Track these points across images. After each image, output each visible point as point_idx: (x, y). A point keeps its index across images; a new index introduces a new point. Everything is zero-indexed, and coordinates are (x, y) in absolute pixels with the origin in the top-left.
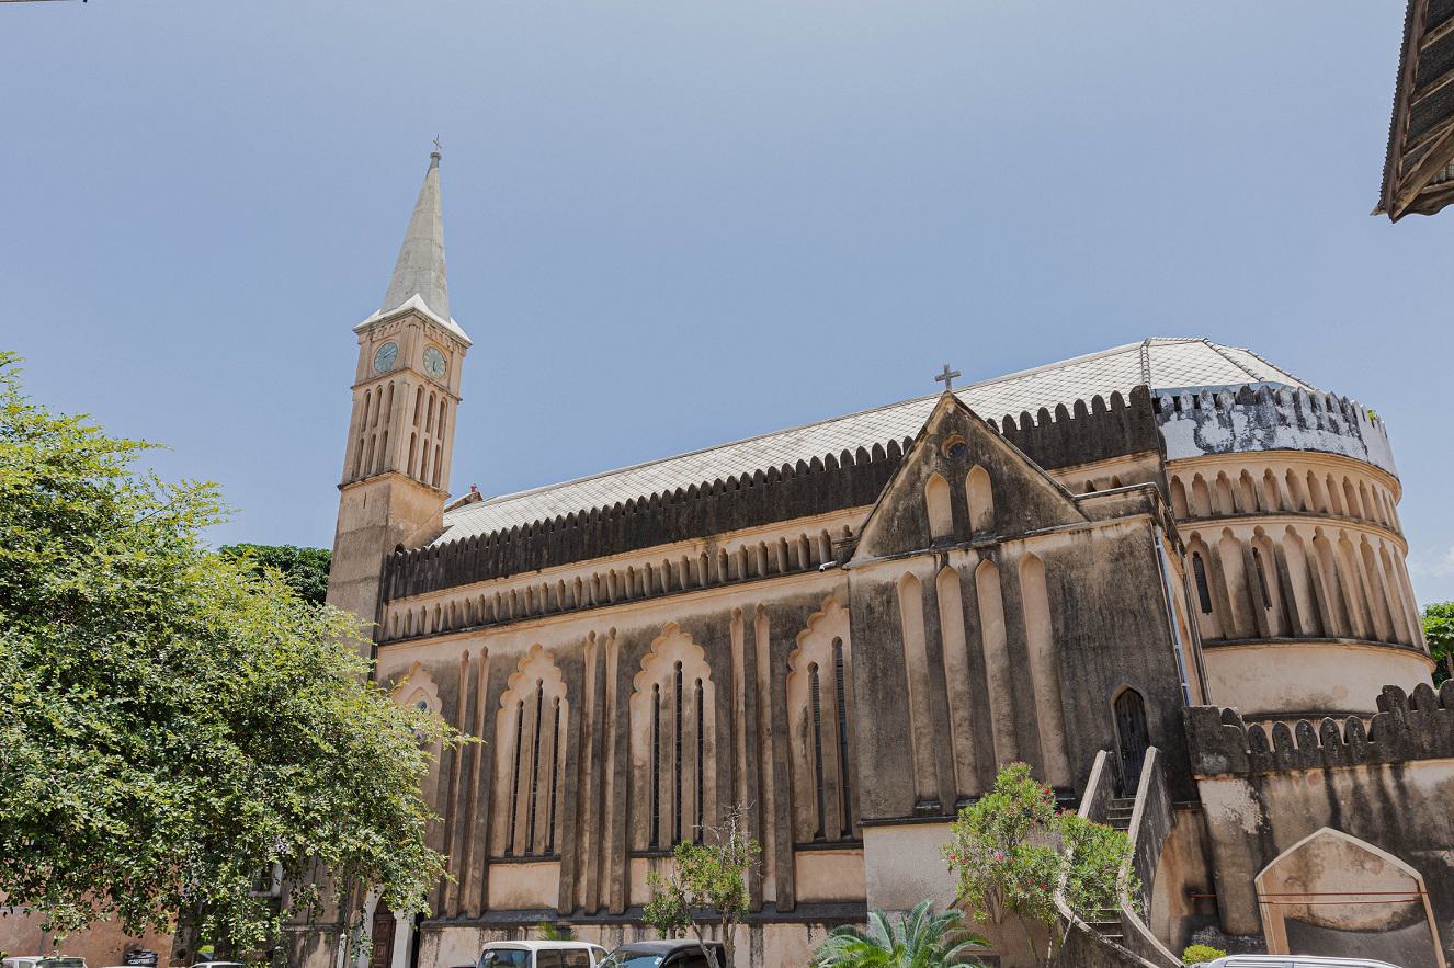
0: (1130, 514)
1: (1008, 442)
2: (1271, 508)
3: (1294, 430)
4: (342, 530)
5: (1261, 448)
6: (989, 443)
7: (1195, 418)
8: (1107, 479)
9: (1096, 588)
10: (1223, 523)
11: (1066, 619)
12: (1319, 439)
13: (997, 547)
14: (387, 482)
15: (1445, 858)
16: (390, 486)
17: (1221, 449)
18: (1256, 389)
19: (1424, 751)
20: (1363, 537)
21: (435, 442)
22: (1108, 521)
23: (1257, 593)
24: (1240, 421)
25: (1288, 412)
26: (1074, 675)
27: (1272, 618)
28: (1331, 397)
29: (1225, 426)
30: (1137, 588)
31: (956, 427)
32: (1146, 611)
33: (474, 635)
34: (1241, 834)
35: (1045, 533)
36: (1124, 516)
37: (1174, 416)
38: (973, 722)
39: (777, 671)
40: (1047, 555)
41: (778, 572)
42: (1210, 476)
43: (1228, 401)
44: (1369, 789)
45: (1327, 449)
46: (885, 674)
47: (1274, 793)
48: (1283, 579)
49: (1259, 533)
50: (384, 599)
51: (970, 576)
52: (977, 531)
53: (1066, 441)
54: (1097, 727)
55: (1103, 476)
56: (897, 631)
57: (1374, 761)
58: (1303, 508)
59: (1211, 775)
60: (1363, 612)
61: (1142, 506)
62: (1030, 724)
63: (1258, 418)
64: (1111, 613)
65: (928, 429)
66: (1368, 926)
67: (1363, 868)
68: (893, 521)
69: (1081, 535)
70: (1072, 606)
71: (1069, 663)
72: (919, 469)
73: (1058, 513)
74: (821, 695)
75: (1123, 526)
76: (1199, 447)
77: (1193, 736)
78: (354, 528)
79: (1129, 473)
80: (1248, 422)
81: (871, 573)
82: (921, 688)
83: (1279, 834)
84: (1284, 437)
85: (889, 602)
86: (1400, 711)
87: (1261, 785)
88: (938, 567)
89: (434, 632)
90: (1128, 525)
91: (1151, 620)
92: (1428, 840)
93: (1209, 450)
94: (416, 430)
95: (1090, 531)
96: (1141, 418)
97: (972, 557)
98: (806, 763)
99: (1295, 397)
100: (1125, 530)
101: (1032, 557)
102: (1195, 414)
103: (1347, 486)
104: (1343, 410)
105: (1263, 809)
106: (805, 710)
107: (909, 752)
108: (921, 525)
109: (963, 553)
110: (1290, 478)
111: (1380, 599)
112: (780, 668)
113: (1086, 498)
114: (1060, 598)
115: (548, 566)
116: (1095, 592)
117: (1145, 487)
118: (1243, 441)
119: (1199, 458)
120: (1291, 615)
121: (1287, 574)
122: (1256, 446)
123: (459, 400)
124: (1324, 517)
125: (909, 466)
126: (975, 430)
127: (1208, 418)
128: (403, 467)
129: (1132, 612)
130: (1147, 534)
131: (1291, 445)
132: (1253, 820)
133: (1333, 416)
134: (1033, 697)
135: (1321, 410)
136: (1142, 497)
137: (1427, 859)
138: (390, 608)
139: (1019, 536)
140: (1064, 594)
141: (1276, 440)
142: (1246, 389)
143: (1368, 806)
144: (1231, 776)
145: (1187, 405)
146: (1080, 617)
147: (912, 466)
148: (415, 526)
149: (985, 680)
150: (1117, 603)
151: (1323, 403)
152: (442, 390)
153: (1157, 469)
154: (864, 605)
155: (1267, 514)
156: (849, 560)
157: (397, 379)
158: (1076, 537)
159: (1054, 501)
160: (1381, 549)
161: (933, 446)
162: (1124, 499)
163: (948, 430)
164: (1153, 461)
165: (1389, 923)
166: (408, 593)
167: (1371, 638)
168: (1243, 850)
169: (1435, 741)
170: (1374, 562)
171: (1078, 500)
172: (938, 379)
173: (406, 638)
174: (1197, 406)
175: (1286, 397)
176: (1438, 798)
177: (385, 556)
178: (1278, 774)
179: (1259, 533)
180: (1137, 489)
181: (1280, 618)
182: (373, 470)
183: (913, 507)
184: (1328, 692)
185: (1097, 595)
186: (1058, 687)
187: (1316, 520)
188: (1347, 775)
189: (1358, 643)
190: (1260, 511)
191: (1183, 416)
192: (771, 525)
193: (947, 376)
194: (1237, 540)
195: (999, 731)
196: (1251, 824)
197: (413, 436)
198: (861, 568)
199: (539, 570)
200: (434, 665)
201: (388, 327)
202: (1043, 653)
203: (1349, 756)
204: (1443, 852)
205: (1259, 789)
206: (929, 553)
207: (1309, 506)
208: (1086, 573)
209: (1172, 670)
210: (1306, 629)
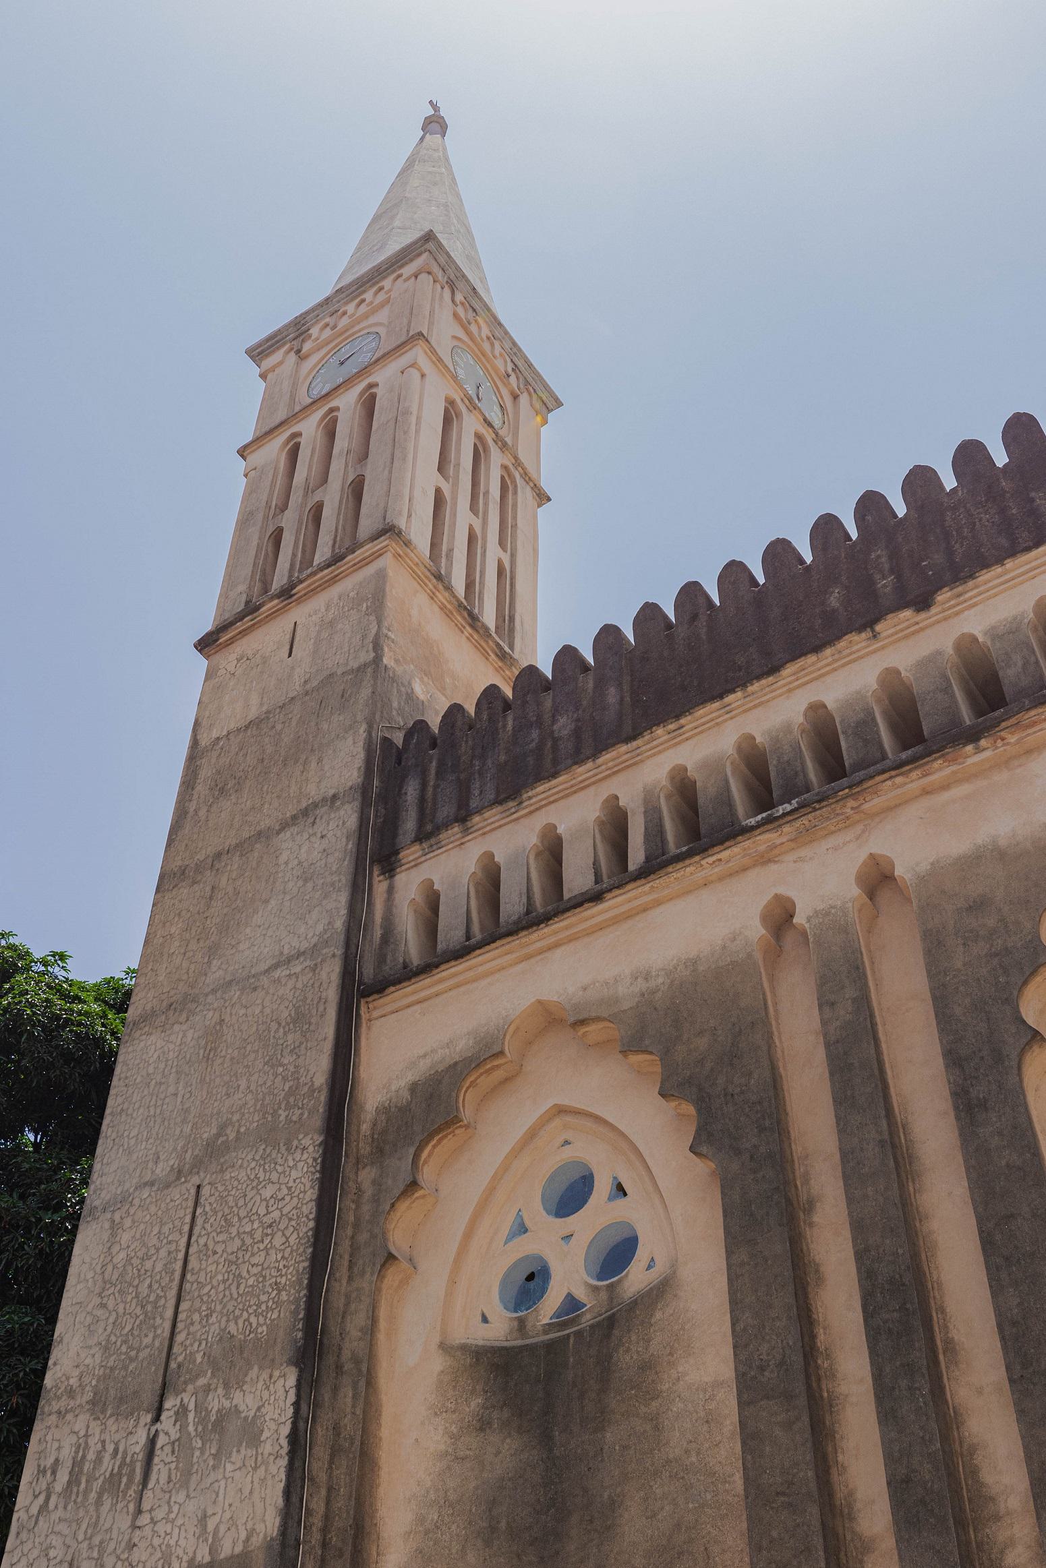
4: (204, 741)
16: (381, 576)
33: (798, 840)
78: (253, 713)
138: (401, 878)
157: (383, 376)
166: (474, 803)
182: (323, 553)
201: (350, 308)
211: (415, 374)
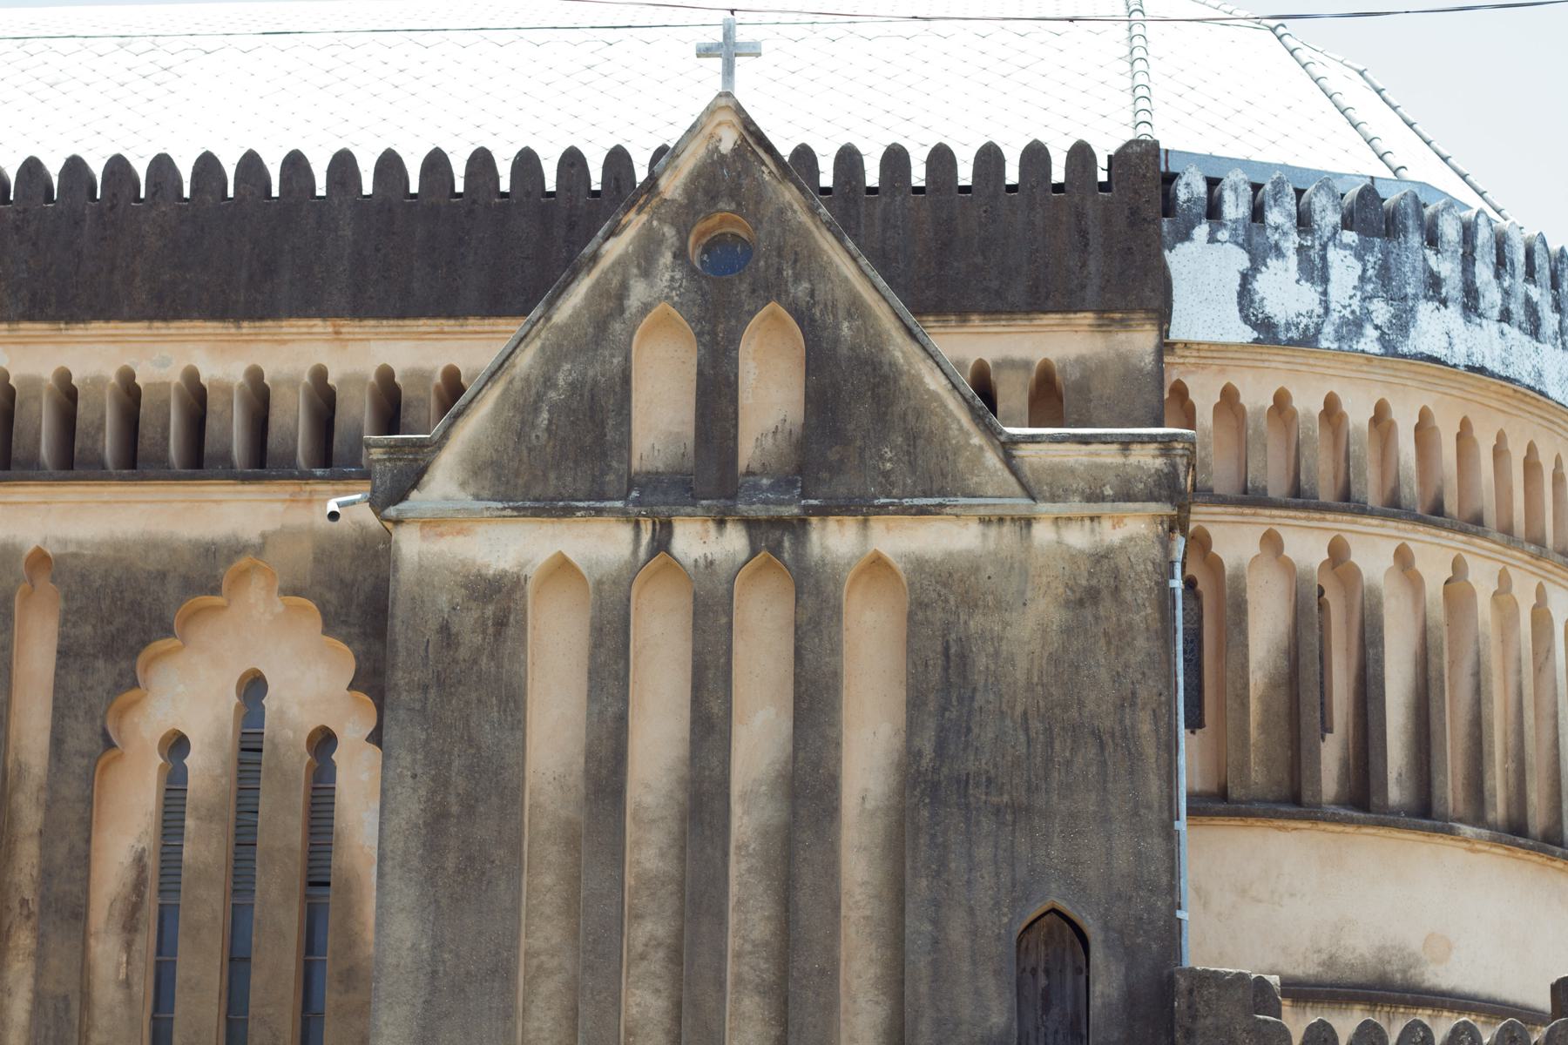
0: (1128, 497)
1: (864, 261)
2: (1373, 498)
3: (1453, 313)
5: (1376, 348)
6: (814, 253)
7: (1247, 245)
8: (1026, 365)
9: (1022, 663)
10: (1267, 518)
11: (941, 729)
12: (1498, 345)
13: (798, 527)
17: (1294, 334)
18: (1391, 196)
20: (1541, 593)
22: (1076, 507)
23: (1310, 696)
24: (1344, 269)
25: (1447, 267)
26: (943, 863)
27: (1331, 754)
28: (1538, 246)
29: (1310, 279)
30: (1117, 678)
31: (734, 193)
32: (1128, 737)
35: (922, 511)
36: (1115, 499)
37: (1202, 231)
38: (677, 955)
39: (72, 744)
40: (919, 565)
41: (103, 466)
42: (1256, 396)
43: (1327, 217)
45: (1510, 373)
46: (469, 810)
48: (1370, 671)
49: (1338, 554)
51: (722, 589)
52: (749, 473)
54: (977, 992)
56: (512, 701)
58: (1437, 509)
60: (1512, 766)
61: (1158, 484)
62: (822, 972)
64: (1049, 730)
65: (663, 183)
68: (536, 410)
69: (1007, 528)
70: (961, 700)
71: (933, 836)
72: (624, 289)
73: (961, 465)
74: (190, 823)
75: (1106, 524)
76: (1246, 319)
77: (1189, 1034)
79: (1081, 361)
80: (1363, 279)
81: (459, 540)
82: (553, 853)
85: (501, 623)
88: (643, 552)
90: (1118, 522)
91: (1134, 758)
93: (1266, 329)
95: (1028, 522)
96: (1132, 224)
97: (734, 541)
98: (130, 1001)
101: (877, 564)
102: (1248, 231)
103: (1531, 465)
106: (139, 861)
107: (508, 1014)
108: (610, 435)
109: (711, 526)
110: (1424, 429)
111: (1547, 735)
112: (81, 736)
113: (1033, 439)
114: (935, 676)
116: (1020, 675)
117: (1173, 438)
118: (1344, 322)
119: (1242, 347)
121: (1380, 662)
122: (1369, 341)
124: (1477, 534)
125: (596, 273)
126: (782, 211)
127: (1279, 253)
129: (1097, 734)
130: (1156, 552)
131: (1439, 350)
133: (1535, 293)
134: (836, 908)
135: (1513, 276)
136: (1159, 463)
139: (859, 507)
140: (946, 669)
141: (1413, 332)
145: (1235, 208)
146: (976, 730)
147: (605, 273)
149: (726, 854)
150: (1066, 708)
151: (1520, 257)
153: (1148, 361)
154: (433, 624)
155: (1362, 510)
156: (403, 497)
158: (993, 531)
159: (954, 430)
161: (669, 232)
162: (1119, 460)
163: (713, 197)
164: (1141, 341)
167: (1515, 831)
170: (1550, 650)
171: (1015, 441)
172: (705, 52)
174: (1257, 213)
175: (1450, 230)
179: (1338, 554)
180: (1152, 439)
181: (1345, 765)
183: (595, 382)
184: (1415, 944)
185: (1022, 681)
186: (897, 893)
187: (1457, 541)
190: (1347, 501)
191: (1223, 235)
192: (97, 328)
193: (727, 51)
194: (1288, 567)
195: (739, 980)
198: (433, 523)
202: (870, 805)
206: (623, 515)
207: (1451, 505)
208: (1006, 624)
209: (1164, 880)
210: (1396, 792)
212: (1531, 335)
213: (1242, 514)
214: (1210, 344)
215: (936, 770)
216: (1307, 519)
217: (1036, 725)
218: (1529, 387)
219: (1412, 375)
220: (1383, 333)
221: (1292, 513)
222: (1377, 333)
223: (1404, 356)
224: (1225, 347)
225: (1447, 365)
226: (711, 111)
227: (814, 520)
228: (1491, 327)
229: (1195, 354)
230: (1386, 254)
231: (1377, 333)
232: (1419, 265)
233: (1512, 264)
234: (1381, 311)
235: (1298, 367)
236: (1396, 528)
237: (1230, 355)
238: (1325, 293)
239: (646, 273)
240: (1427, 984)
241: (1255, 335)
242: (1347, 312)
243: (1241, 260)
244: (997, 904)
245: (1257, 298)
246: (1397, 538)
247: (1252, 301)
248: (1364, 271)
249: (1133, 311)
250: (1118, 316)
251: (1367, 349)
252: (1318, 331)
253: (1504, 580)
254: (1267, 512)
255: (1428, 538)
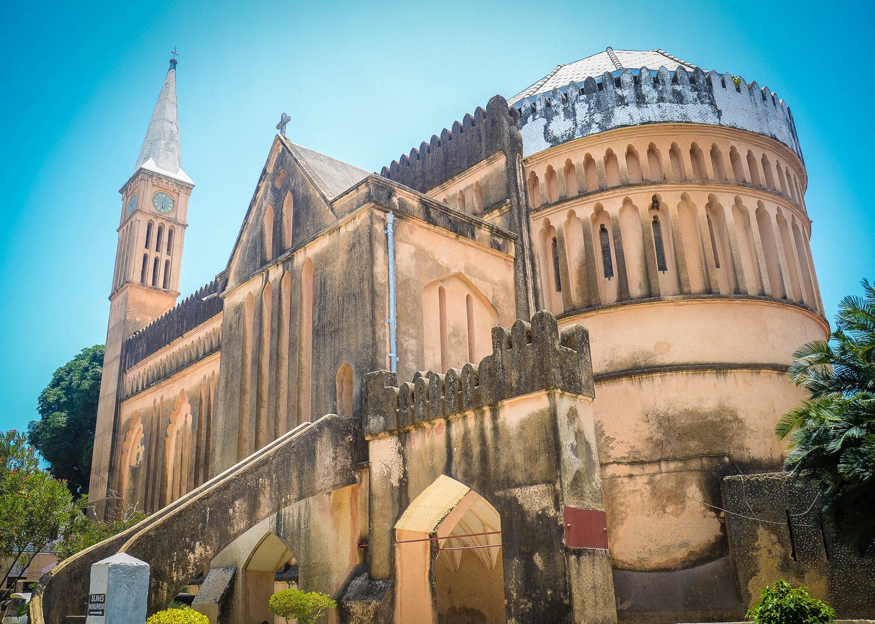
0: (359, 206)
3: (632, 108)
5: (598, 131)
8: (472, 186)
10: (567, 207)
12: (657, 112)
14: (126, 291)
15: (517, 497)
16: (127, 294)
17: (565, 138)
19: (512, 390)
21: (164, 257)
22: (348, 216)
24: (581, 110)
25: (628, 93)
29: (569, 117)
32: (362, 292)
33: (158, 388)
34: (389, 487)
36: (357, 208)
37: (530, 119)
40: (316, 256)
42: (559, 165)
44: (474, 435)
45: (666, 119)
47: (413, 447)
50: (123, 371)
53: (446, 159)
55: (469, 184)
57: (478, 409)
59: (375, 435)
60: (704, 268)
61: (366, 197)
63: (598, 104)
66: (663, 566)
67: (665, 512)
69: (335, 233)
75: (357, 218)
76: (547, 141)
80: (589, 109)
83: (411, 486)
84: (621, 116)
86: (499, 352)
87: (406, 439)
89: (143, 389)
91: (363, 299)
92: (508, 478)
93: (554, 141)
94: (147, 251)
99: (637, 81)
100: (358, 221)
102: (545, 111)
104: (692, 81)
105: (405, 462)
114: (318, 293)
115: (186, 332)
116: (337, 283)
118: (583, 126)
119: (548, 150)
120: (653, 282)
122: (595, 129)
123: (185, 226)
127: (557, 113)
128: (136, 277)
130: (369, 222)
132: (397, 474)
133: (678, 88)
137: (505, 498)
142: (590, 80)
143: (471, 450)
144: (387, 434)
145: (539, 107)
148: (150, 318)
152: (169, 220)
156: (224, 290)
160: (757, 211)
165: (685, 562)
168: (388, 503)
169: (520, 377)
173: (134, 394)
174: (548, 105)
175: (627, 79)
176: (520, 435)
177: (124, 341)
178: (416, 428)
182: (121, 283)
188: (461, 422)
189: (684, 299)
194: (579, 219)
196: (395, 481)
197: (145, 257)
199: (182, 335)
200: (143, 411)
203: (460, 402)
204: (517, 490)
205: (403, 445)
211: (138, 222)
212: (678, 102)
213: (558, 208)
214: (538, 154)
215: (318, 325)
216: (583, 201)
217: (341, 298)
218: (678, 122)
219: (620, 135)
220: (600, 124)
221: (576, 201)
222: (598, 125)
223: (610, 129)
224: (543, 153)
225: (631, 126)
226: (275, 142)
227: (295, 253)
228: (655, 106)
229: (535, 160)
230: (598, 97)
231: (598, 125)
232: (613, 95)
233: (663, 81)
234: (598, 117)
235: (573, 149)
236: (621, 192)
237: (547, 155)
238: (575, 120)
239: (266, 198)
240: (658, 363)
241: (551, 144)
242: (584, 123)
243: (544, 121)
244: (330, 369)
245: (550, 132)
246: (623, 195)
247: (549, 134)
248: (590, 106)
249: (495, 153)
250: (492, 157)
251: (594, 132)
252: (574, 133)
253: (737, 201)
254: (566, 204)
255: (637, 191)
